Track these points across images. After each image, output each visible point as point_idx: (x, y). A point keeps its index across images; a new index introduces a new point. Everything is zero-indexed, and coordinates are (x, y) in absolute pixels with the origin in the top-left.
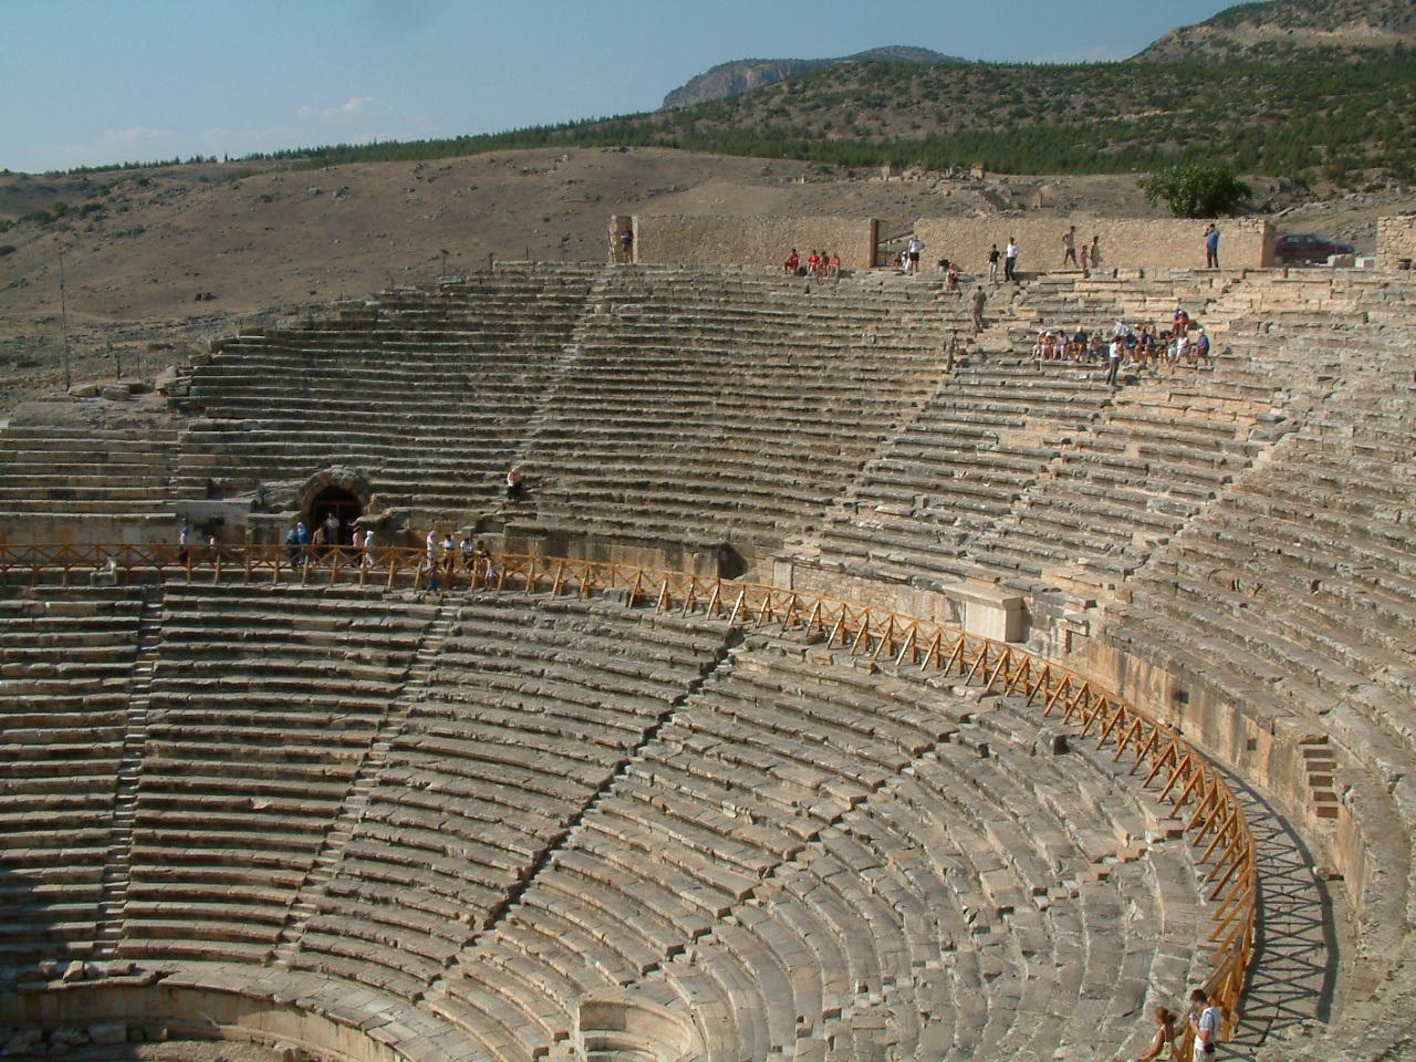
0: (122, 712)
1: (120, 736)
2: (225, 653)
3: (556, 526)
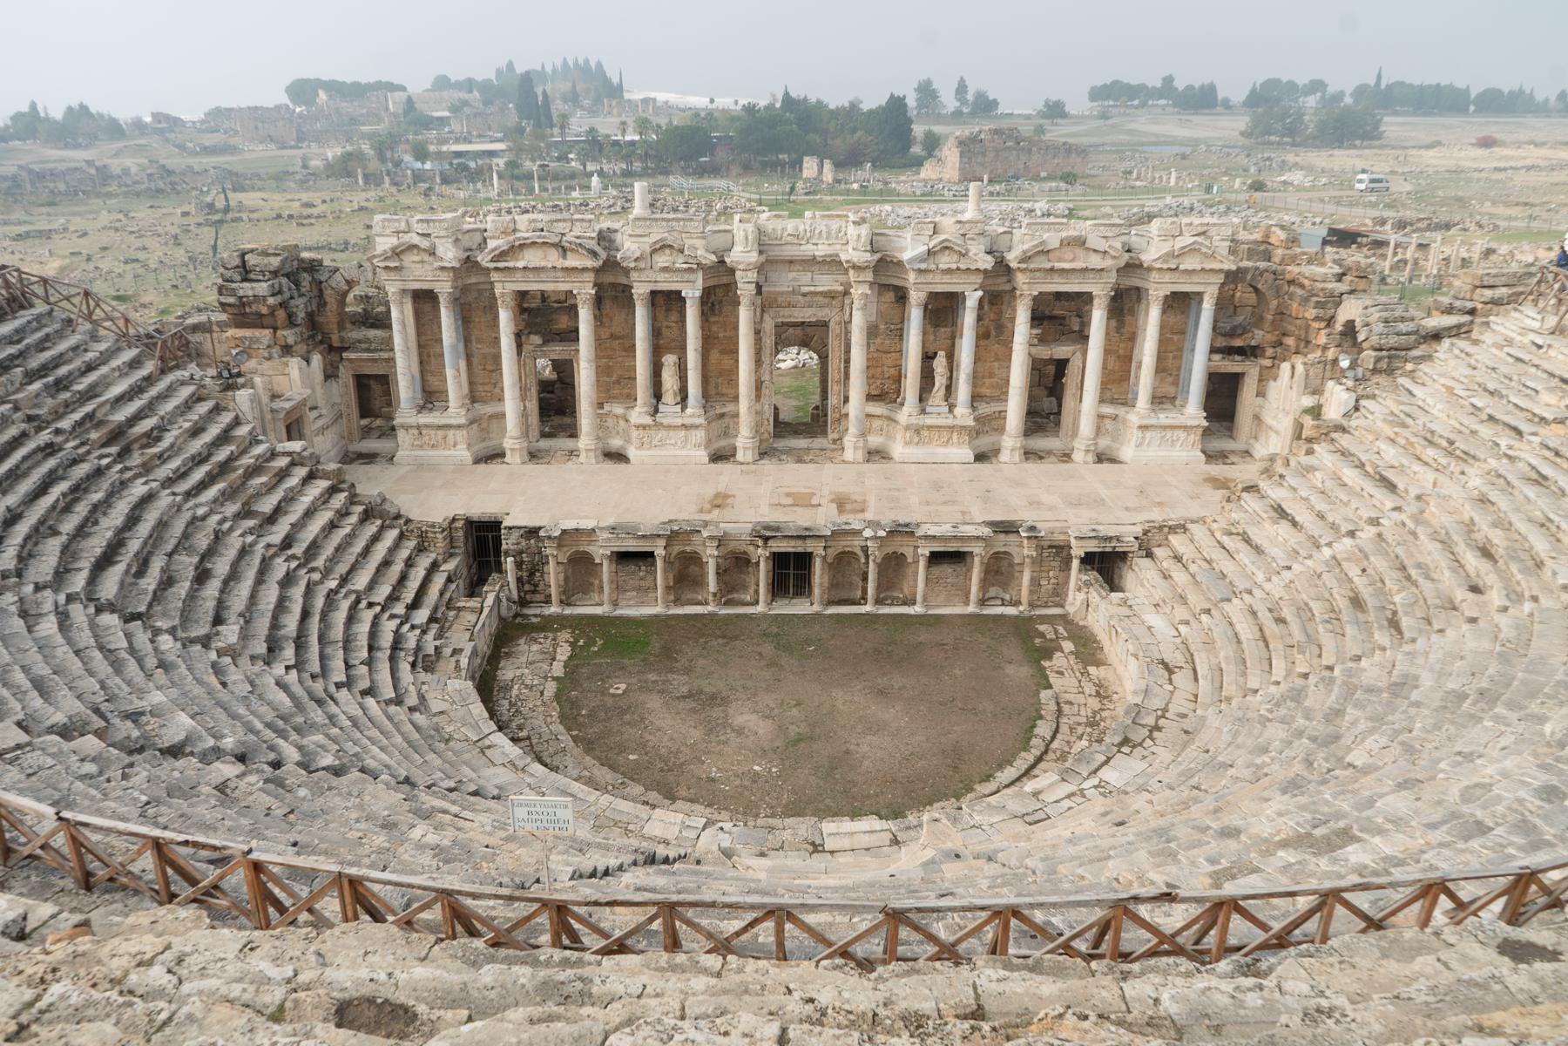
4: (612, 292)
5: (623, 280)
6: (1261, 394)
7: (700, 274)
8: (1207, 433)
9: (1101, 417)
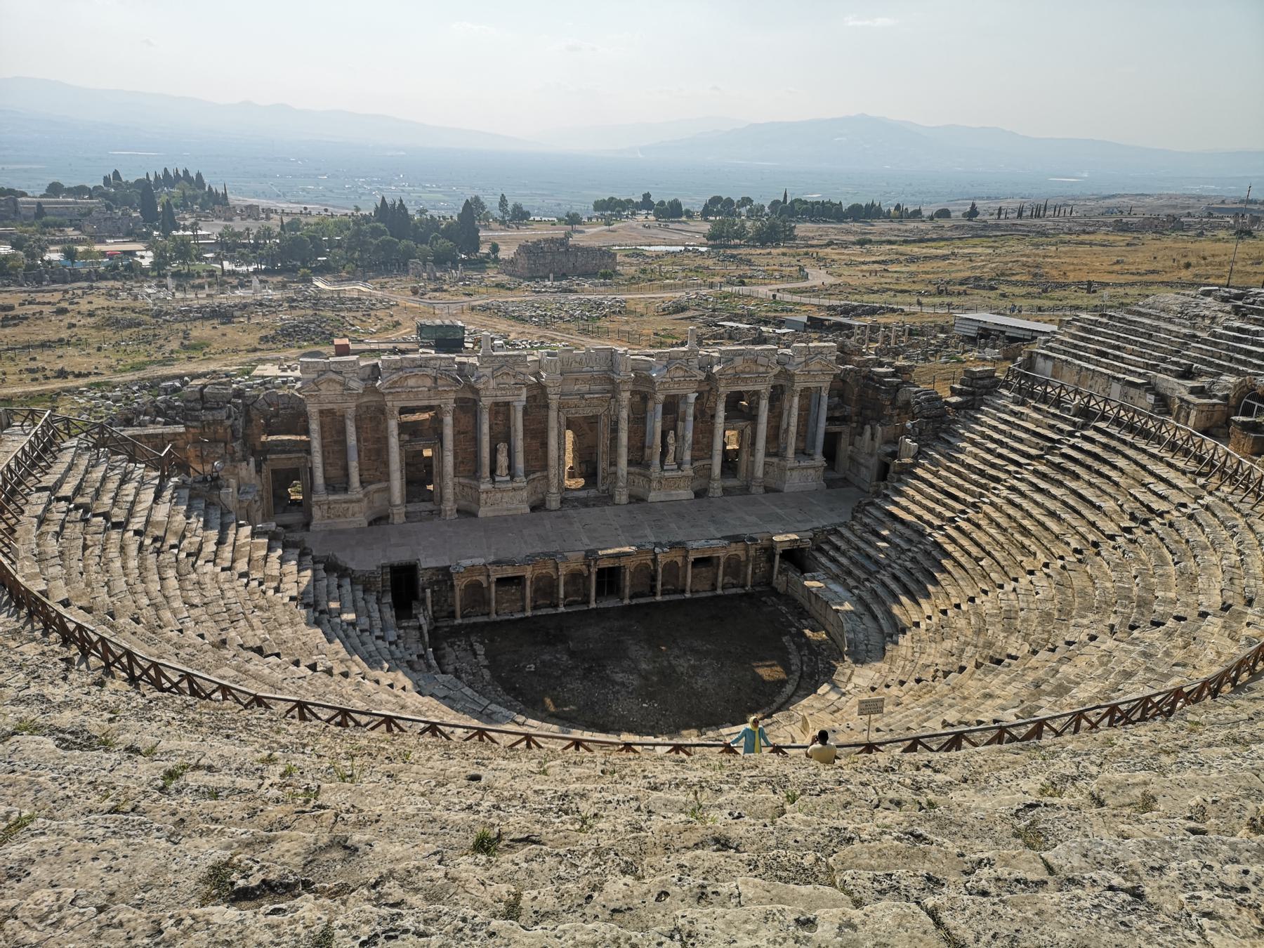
4: (468, 406)
5: (470, 395)
6: (852, 444)
7: (524, 390)
8: (826, 469)
9: (765, 464)
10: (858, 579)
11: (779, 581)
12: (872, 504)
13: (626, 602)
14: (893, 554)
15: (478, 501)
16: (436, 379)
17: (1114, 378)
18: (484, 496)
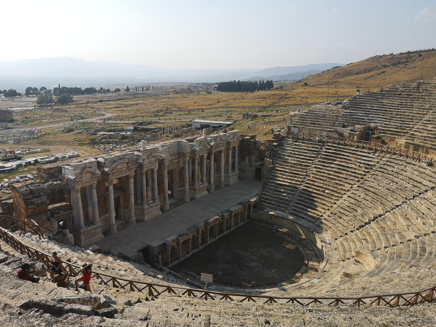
0: (308, 168)
1: (306, 172)
2: (333, 160)
3: (418, 143)
10: (285, 207)
11: (253, 215)
12: (268, 182)
13: (217, 238)
14: (291, 197)
15: (143, 214)
16: (128, 163)
17: (323, 130)
18: (146, 211)
